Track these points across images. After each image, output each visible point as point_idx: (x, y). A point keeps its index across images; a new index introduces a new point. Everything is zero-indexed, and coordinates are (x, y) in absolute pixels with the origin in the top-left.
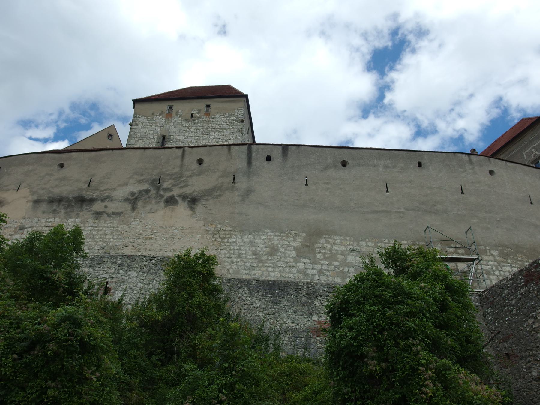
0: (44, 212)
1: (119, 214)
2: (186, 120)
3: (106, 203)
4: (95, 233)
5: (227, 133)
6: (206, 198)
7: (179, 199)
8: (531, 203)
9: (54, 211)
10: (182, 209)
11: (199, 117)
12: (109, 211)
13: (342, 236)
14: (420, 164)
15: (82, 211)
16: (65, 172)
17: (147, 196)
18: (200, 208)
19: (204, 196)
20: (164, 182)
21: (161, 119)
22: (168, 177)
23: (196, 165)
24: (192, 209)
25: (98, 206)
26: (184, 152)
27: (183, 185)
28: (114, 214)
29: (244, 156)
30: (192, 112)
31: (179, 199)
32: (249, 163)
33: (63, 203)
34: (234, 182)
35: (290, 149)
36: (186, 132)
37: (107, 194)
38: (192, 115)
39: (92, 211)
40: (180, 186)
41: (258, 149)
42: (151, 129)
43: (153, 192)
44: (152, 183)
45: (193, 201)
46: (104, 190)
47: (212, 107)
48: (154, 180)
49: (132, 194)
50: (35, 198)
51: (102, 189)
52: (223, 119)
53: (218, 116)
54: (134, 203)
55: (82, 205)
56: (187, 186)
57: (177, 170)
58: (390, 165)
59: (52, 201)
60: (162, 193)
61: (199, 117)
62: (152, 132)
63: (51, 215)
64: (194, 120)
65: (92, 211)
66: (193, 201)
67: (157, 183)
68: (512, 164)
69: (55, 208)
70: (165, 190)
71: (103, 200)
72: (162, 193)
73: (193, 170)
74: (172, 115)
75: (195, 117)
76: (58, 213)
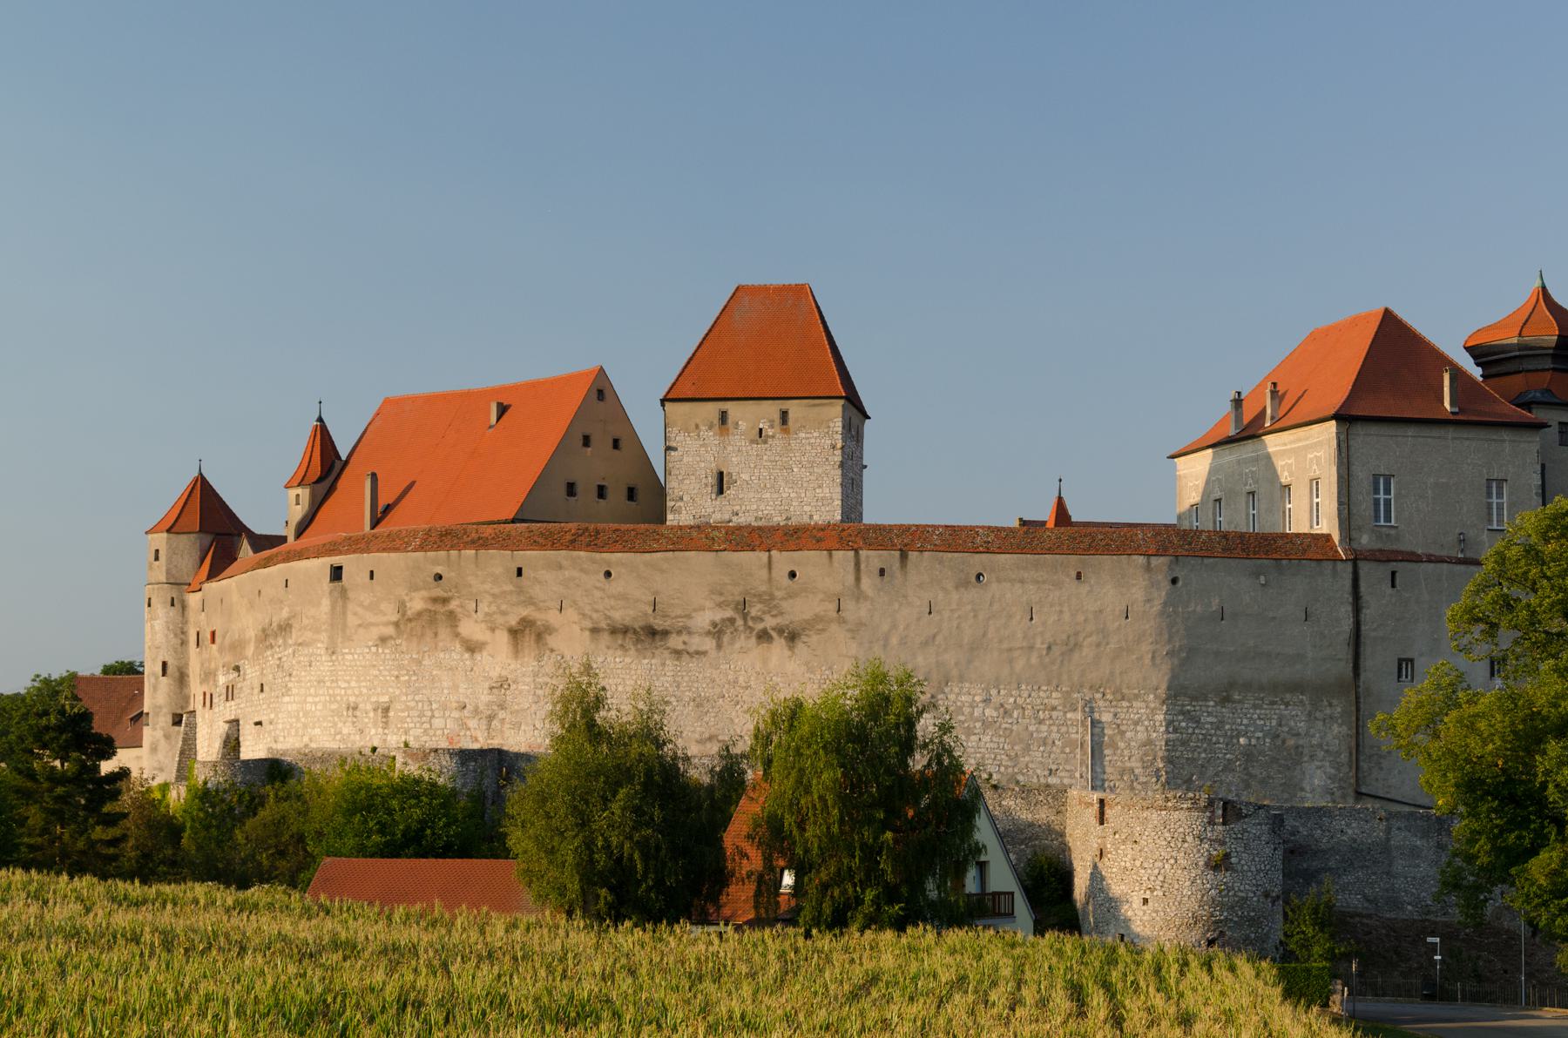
0: (608, 648)
1: (704, 653)
2: (752, 442)
3: (685, 637)
4: (679, 679)
5: (820, 471)
6: (807, 632)
7: (774, 634)
8: (1222, 619)
9: (622, 646)
10: (779, 644)
11: (773, 437)
12: (691, 650)
13: (971, 683)
14: (1079, 576)
15: (657, 648)
16: (616, 586)
17: (732, 630)
18: (800, 646)
19: (804, 629)
20: (750, 606)
21: (710, 436)
22: (755, 600)
23: (786, 581)
24: (791, 648)
25: (675, 642)
26: (770, 557)
27: (774, 613)
28: (698, 653)
29: (851, 567)
30: (761, 426)
31: (774, 634)
32: (858, 579)
33: (629, 635)
34: (839, 610)
35: (910, 557)
36: (755, 467)
37: (681, 624)
38: (761, 430)
39: (668, 648)
40: (773, 613)
41: (868, 557)
42: (698, 459)
43: (740, 622)
44: (736, 609)
45: (792, 637)
46: (677, 617)
47: (791, 415)
48: (738, 604)
49: (715, 625)
50: (589, 624)
51: (673, 615)
52: (813, 441)
53: (802, 435)
54: (719, 638)
55: (654, 640)
56: (782, 614)
57: (763, 588)
58: (1040, 579)
59: (614, 631)
60: (750, 623)
61: (773, 437)
62: (703, 465)
63: (619, 652)
64: (765, 442)
65: (668, 648)
66: (792, 637)
67: (742, 607)
68: (1211, 560)
69: (620, 642)
70: (754, 619)
71: (679, 632)
72: (750, 623)
73: (785, 589)
74: (728, 430)
75: (767, 436)
76: (627, 650)
